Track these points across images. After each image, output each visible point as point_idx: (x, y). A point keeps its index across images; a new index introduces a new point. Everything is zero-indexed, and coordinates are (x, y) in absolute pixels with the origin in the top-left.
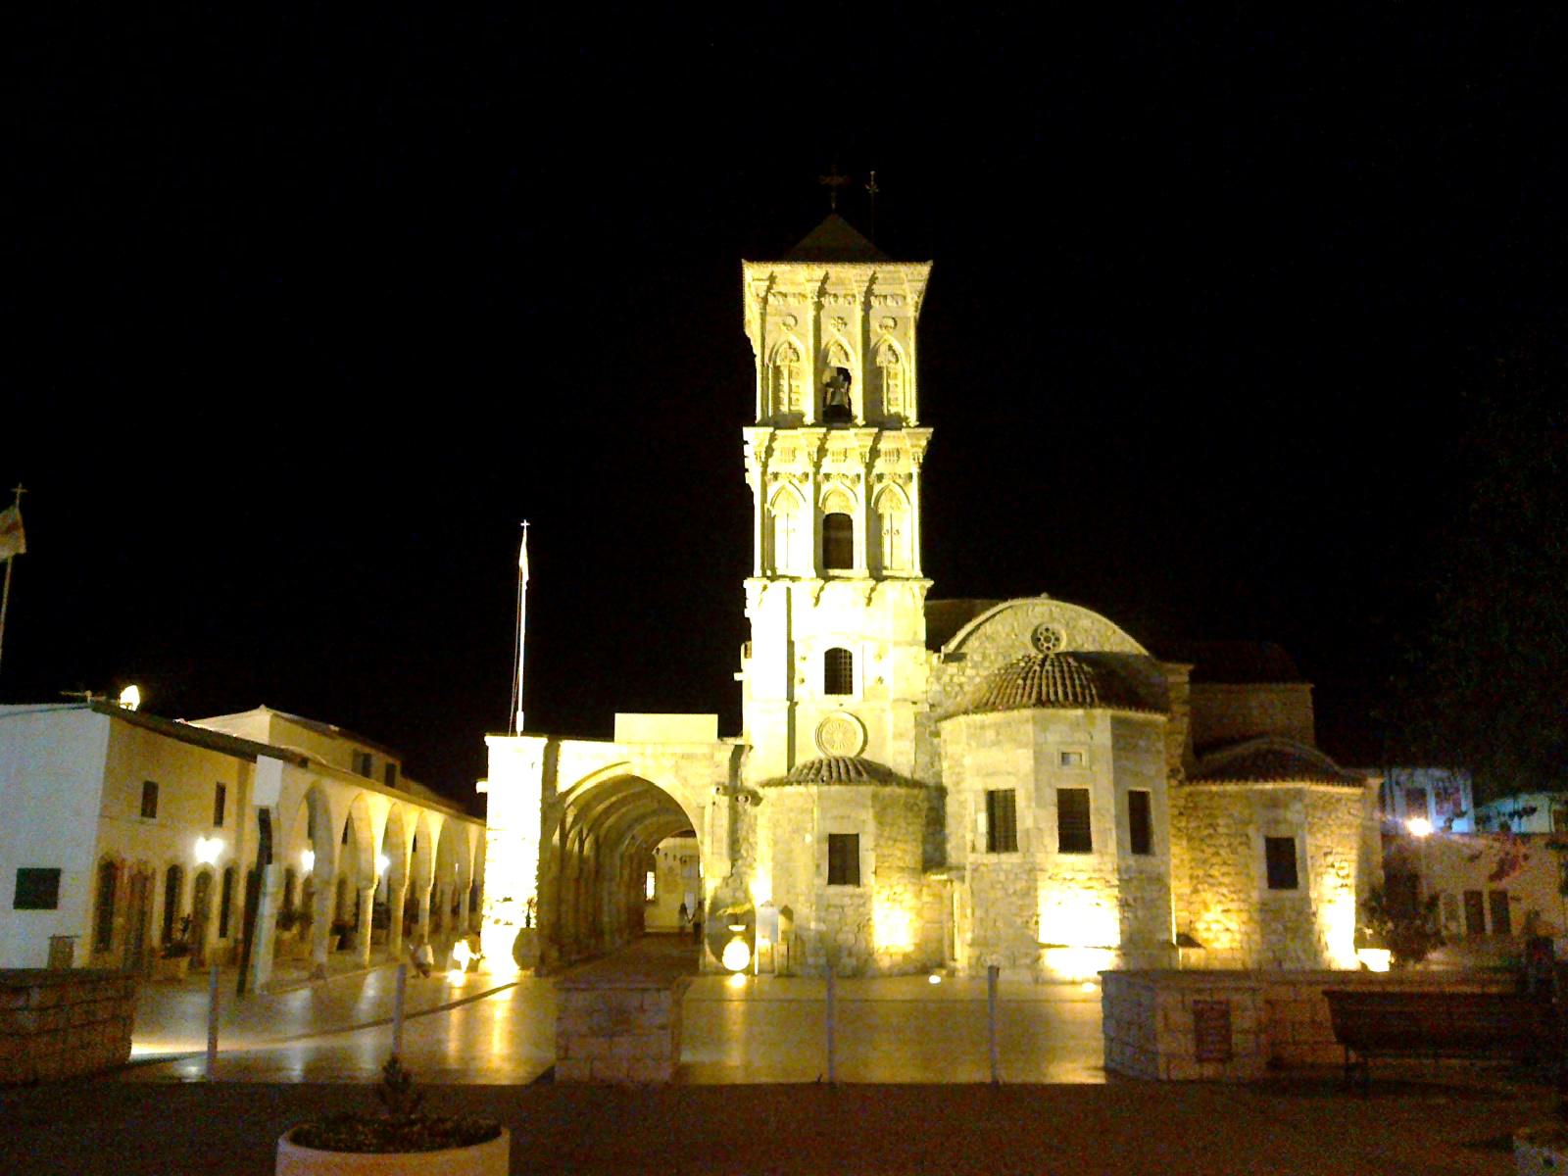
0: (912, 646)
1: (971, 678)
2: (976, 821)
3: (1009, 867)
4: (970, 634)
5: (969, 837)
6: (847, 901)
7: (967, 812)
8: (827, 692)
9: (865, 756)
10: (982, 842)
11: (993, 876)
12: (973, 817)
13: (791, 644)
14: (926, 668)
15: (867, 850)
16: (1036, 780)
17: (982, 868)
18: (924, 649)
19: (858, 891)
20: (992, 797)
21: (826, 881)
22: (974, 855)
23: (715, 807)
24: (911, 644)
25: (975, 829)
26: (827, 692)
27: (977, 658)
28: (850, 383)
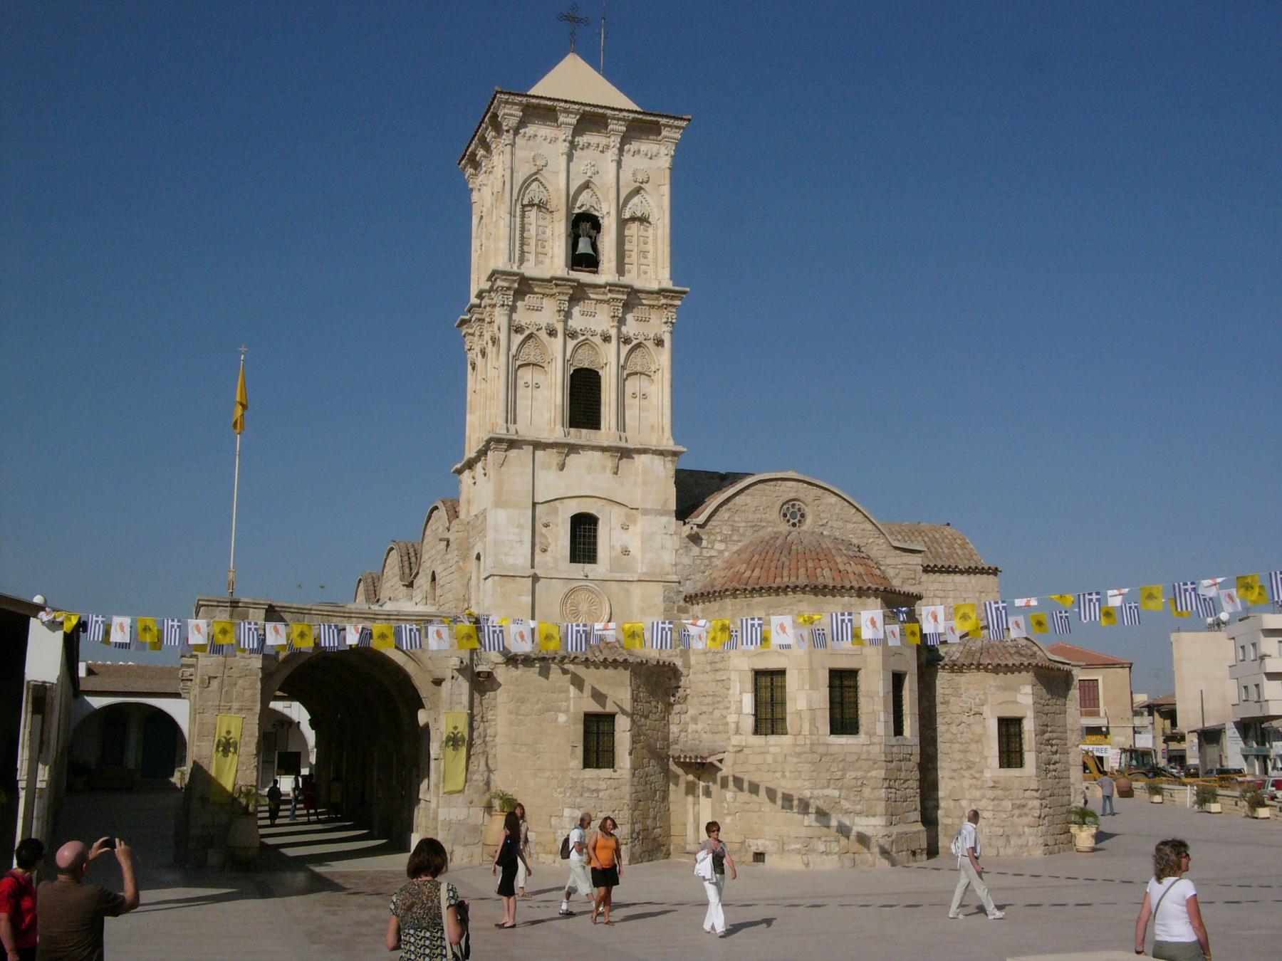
0: (661, 515)
1: (721, 552)
2: (741, 701)
4: (721, 505)
5: (732, 718)
6: (603, 785)
7: (731, 692)
8: (571, 562)
10: (749, 723)
11: (759, 759)
13: (534, 504)
15: (624, 731)
16: (811, 664)
17: (746, 751)
18: (675, 519)
20: (758, 674)
21: (581, 766)
22: (738, 737)
23: (454, 680)
24: (663, 513)
26: (572, 561)
27: (727, 531)
28: (599, 232)
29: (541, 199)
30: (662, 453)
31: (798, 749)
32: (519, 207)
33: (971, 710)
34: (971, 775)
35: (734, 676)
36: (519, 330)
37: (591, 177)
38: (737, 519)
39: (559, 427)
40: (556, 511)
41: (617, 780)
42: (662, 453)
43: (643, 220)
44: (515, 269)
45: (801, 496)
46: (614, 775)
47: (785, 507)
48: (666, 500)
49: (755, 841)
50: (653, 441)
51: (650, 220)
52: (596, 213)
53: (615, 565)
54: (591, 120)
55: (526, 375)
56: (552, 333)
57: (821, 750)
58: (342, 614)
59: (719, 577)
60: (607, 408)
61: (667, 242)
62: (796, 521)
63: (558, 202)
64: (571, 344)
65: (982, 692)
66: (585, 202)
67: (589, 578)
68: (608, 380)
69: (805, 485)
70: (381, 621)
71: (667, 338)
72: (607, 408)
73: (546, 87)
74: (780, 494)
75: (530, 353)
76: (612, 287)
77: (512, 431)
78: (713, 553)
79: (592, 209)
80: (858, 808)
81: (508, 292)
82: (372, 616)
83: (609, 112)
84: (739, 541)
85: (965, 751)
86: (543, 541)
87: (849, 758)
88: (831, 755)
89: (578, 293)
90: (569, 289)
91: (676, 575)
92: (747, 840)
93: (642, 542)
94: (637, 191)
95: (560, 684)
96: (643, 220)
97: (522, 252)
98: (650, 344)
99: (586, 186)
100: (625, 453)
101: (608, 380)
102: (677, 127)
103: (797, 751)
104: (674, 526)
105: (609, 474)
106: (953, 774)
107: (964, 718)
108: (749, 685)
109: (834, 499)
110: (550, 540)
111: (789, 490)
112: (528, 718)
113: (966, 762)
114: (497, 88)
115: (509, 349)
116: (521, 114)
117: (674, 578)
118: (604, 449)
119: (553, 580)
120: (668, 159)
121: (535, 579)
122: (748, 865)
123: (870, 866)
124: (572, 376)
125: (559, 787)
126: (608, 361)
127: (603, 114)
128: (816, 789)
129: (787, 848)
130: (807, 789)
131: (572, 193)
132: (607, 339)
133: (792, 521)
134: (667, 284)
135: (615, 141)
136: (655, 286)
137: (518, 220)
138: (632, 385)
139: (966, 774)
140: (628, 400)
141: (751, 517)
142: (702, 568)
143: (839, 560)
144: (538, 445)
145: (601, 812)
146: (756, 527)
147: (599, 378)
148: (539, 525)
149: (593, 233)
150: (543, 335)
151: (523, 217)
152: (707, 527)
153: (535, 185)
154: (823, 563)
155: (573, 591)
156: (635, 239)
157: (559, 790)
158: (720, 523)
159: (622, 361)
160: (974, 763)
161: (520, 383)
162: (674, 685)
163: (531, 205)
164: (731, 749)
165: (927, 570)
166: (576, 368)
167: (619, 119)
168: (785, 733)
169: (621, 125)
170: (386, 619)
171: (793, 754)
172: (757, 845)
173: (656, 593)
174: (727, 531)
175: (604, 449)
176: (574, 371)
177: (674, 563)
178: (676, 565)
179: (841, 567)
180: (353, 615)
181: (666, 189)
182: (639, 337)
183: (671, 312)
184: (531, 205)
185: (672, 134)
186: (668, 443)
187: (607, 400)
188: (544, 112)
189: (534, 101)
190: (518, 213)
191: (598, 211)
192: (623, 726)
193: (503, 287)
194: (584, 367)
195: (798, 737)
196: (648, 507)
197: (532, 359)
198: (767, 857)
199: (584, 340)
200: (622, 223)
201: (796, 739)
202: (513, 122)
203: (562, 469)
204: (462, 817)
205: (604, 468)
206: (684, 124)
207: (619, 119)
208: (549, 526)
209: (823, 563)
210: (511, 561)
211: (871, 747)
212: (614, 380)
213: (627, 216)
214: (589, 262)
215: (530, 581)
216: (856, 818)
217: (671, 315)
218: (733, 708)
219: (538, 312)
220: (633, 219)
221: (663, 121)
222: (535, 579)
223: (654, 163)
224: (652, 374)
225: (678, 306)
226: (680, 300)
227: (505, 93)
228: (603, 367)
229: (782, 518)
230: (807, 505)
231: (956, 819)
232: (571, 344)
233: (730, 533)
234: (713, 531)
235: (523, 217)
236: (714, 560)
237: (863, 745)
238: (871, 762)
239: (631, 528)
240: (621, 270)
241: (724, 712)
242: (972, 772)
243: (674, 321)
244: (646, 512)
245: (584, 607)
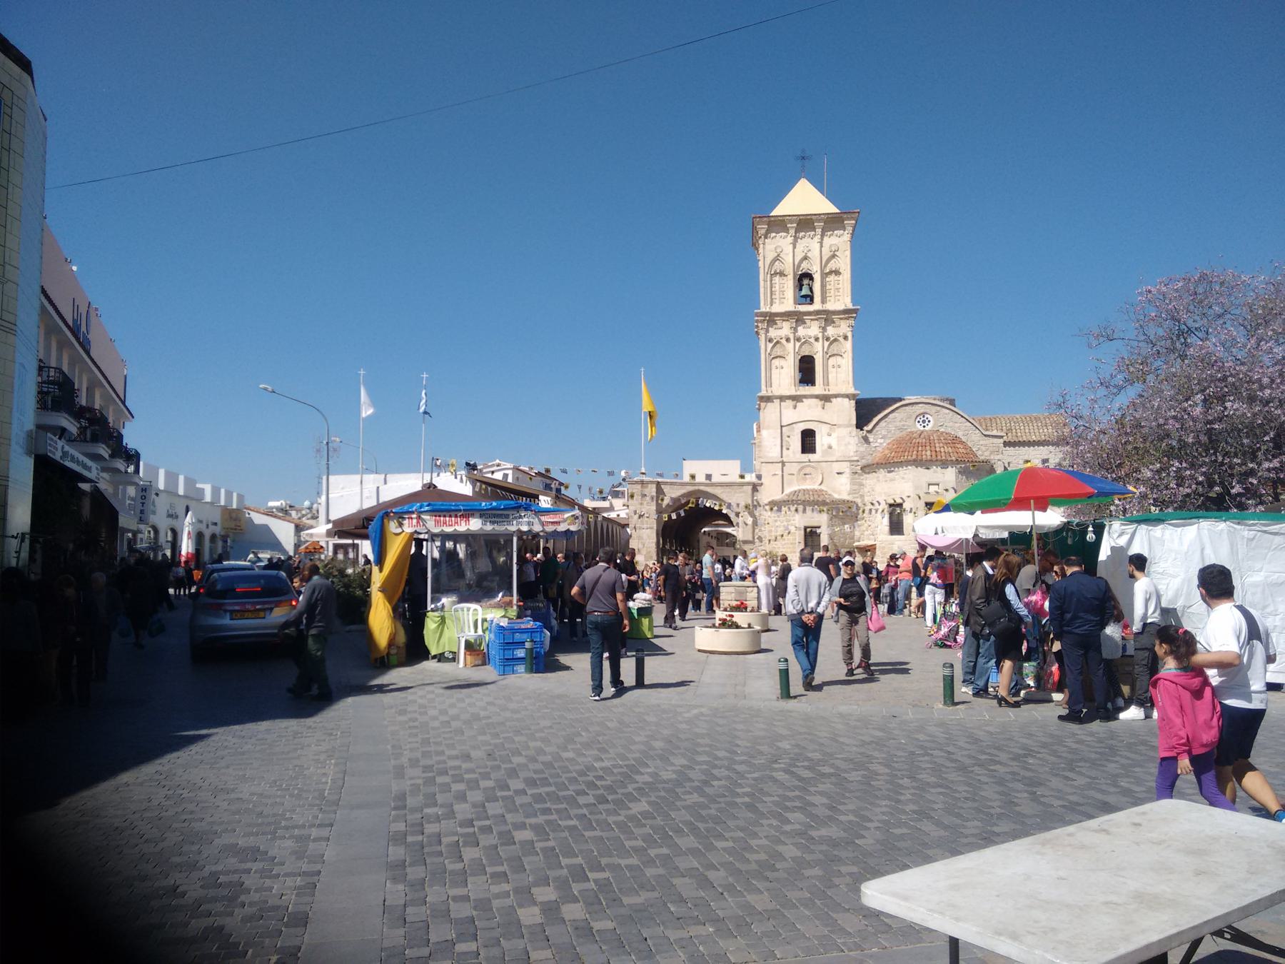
1: (881, 444)
13: (782, 427)
14: (856, 438)
30: (847, 396)
32: (769, 275)
36: (770, 341)
39: (793, 387)
42: (847, 396)
43: (837, 272)
44: (768, 310)
45: (928, 411)
48: (850, 420)
50: (843, 391)
53: (825, 453)
54: (805, 223)
55: (776, 362)
56: (788, 340)
59: (877, 457)
61: (849, 282)
63: (789, 270)
64: (798, 344)
66: (805, 267)
71: (849, 335)
73: (780, 210)
75: (778, 351)
76: (818, 312)
77: (769, 391)
78: (878, 445)
83: (813, 217)
89: (798, 318)
93: (838, 441)
94: (834, 256)
96: (837, 272)
97: (772, 299)
98: (841, 339)
99: (805, 258)
100: (826, 398)
105: (821, 409)
110: (791, 443)
111: (919, 409)
114: (753, 216)
115: (766, 350)
117: (856, 458)
118: (817, 397)
120: (849, 235)
121: (783, 463)
126: (818, 351)
131: (796, 263)
134: (850, 306)
135: (819, 231)
136: (841, 307)
137: (769, 283)
138: (832, 361)
140: (830, 369)
141: (898, 424)
143: (937, 445)
144: (782, 398)
146: (901, 429)
148: (784, 437)
150: (784, 341)
151: (771, 281)
152: (874, 431)
153: (777, 263)
154: (928, 448)
156: (832, 283)
159: (825, 350)
161: (773, 367)
163: (776, 273)
165: (1006, 444)
174: (884, 432)
175: (817, 397)
178: (857, 451)
179: (938, 449)
181: (848, 253)
184: (776, 273)
186: (852, 390)
188: (779, 225)
189: (772, 219)
190: (769, 279)
197: (779, 354)
200: (825, 275)
202: (762, 232)
209: (928, 448)
210: (771, 455)
212: (821, 360)
213: (828, 271)
214: (810, 298)
215: (780, 464)
217: (852, 322)
220: (831, 272)
222: (783, 463)
223: (841, 239)
232: (798, 344)
235: (771, 281)
240: (823, 301)
244: (840, 426)
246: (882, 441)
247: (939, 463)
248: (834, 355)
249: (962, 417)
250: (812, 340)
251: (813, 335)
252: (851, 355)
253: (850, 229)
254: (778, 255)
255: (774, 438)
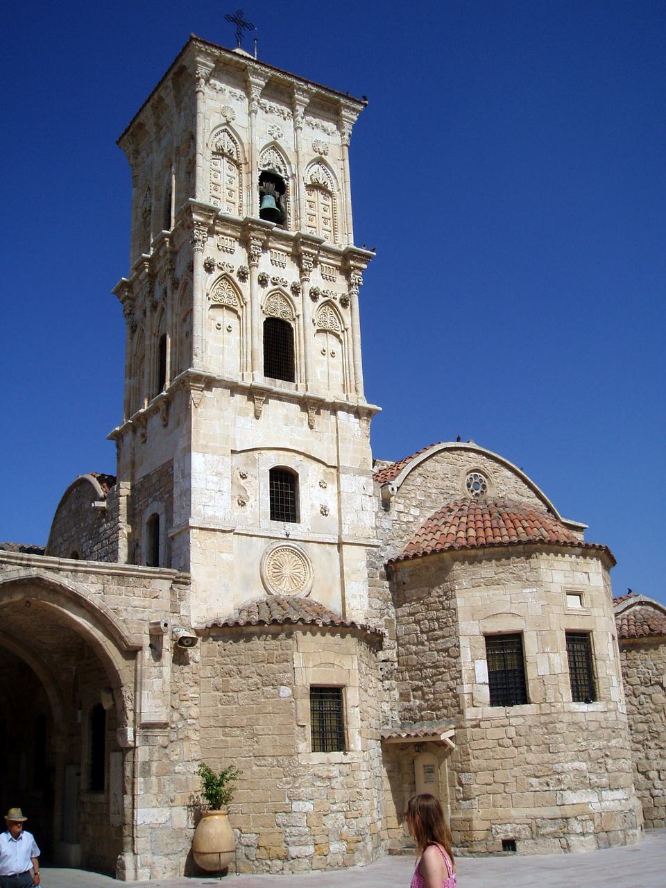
1: (416, 517)
2: (474, 670)
3: (520, 721)
6: (335, 771)
7: (462, 659)
9: (315, 597)
10: (485, 693)
11: (499, 733)
12: (470, 666)
14: (375, 500)
19: (346, 759)
24: (362, 472)
25: (473, 681)
29: (230, 150)
30: (357, 412)
31: (543, 719)
33: (650, 680)
34: (656, 745)
35: (464, 642)
37: (275, 139)
38: (429, 485)
40: (254, 462)
41: (348, 765)
46: (346, 759)
47: (469, 477)
49: (504, 827)
51: (330, 188)
52: (283, 175)
57: (566, 718)
58: (19, 561)
60: (303, 360)
62: (478, 491)
65: (660, 662)
67: (289, 538)
68: (302, 332)
69: (484, 457)
70: (65, 573)
71: (355, 300)
72: (303, 360)
74: (464, 463)
79: (277, 170)
80: (604, 781)
81: (202, 228)
82: (57, 566)
84: (431, 508)
85: (647, 722)
86: (243, 494)
87: (593, 726)
88: (576, 724)
90: (262, 234)
91: (377, 539)
92: (493, 826)
94: (320, 161)
95: (281, 652)
101: (302, 332)
102: (354, 110)
103: (542, 722)
104: (372, 487)
106: (639, 746)
107: (643, 689)
108: (482, 651)
109: (509, 474)
112: (240, 694)
113: (650, 732)
114: (194, 36)
116: (214, 65)
117: (375, 542)
119: (254, 538)
122: (498, 856)
123: (622, 845)
124: (264, 323)
125: (285, 776)
127: (289, 82)
128: (567, 762)
129: (542, 831)
130: (557, 763)
132: (296, 290)
133: (476, 492)
139: (652, 744)
142: (401, 533)
144: (234, 388)
145: (335, 803)
147: (292, 330)
149: (277, 194)
155: (277, 551)
157: (285, 779)
158: (414, 488)
160: (658, 733)
162: (383, 659)
164: (468, 724)
166: (268, 316)
167: (304, 91)
168: (525, 700)
169: (306, 97)
170: (72, 571)
171: (539, 724)
172: (506, 831)
173: (356, 559)
176: (266, 319)
177: (374, 526)
178: (377, 527)
180: (33, 563)
182: (329, 295)
183: (357, 275)
185: (350, 117)
187: (302, 352)
191: (280, 171)
192: (352, 698)
193: (198, 222)
194: (276, 316)
195: (542, 705)
196: (348, 465)
198: (518, 844)
199: (276, 290)
201: (540, 708)
203: (257, 417)
204: (162, 820)
205: (302, 420)
206: (361, 108)
207: (304, 91)
208: (246, 478)
210: (210, 512)
211: (608, 714)
216: (603, 792)
218: (465, 677)
219: (229, 254)
221: (343, 101)
224: (340, 333)
225: (364, 269)
226: (366, 264)
227: (201, 42)
228: (294, 320)
229: (466, 487)
230: (487, 477)
231: (644, 791)
233: (423, 499)
234: (408, 495)
236: (412, 525)
237: (602, 712)
238: (610, 730)
239: (329, 486)
241: (452, 684)
242: (656, 741)
243: (361, 283)
244: (347, 470)
245: (287, 570)
246: (416, 512)
247: (579, 550)
248: (325, 331)
249: (530, 487)
250: (288, 290)
251: (290, 283)
252: (358, 336)
253: (348, 128)
254: (228, 123)
255: (218, 474)
